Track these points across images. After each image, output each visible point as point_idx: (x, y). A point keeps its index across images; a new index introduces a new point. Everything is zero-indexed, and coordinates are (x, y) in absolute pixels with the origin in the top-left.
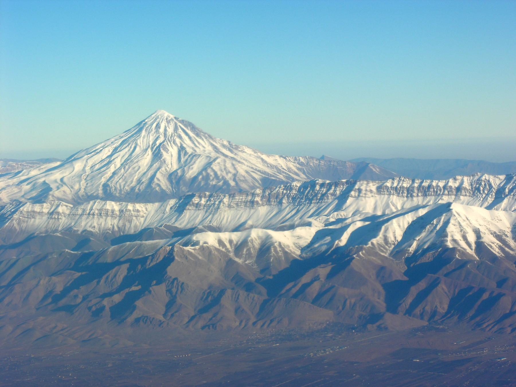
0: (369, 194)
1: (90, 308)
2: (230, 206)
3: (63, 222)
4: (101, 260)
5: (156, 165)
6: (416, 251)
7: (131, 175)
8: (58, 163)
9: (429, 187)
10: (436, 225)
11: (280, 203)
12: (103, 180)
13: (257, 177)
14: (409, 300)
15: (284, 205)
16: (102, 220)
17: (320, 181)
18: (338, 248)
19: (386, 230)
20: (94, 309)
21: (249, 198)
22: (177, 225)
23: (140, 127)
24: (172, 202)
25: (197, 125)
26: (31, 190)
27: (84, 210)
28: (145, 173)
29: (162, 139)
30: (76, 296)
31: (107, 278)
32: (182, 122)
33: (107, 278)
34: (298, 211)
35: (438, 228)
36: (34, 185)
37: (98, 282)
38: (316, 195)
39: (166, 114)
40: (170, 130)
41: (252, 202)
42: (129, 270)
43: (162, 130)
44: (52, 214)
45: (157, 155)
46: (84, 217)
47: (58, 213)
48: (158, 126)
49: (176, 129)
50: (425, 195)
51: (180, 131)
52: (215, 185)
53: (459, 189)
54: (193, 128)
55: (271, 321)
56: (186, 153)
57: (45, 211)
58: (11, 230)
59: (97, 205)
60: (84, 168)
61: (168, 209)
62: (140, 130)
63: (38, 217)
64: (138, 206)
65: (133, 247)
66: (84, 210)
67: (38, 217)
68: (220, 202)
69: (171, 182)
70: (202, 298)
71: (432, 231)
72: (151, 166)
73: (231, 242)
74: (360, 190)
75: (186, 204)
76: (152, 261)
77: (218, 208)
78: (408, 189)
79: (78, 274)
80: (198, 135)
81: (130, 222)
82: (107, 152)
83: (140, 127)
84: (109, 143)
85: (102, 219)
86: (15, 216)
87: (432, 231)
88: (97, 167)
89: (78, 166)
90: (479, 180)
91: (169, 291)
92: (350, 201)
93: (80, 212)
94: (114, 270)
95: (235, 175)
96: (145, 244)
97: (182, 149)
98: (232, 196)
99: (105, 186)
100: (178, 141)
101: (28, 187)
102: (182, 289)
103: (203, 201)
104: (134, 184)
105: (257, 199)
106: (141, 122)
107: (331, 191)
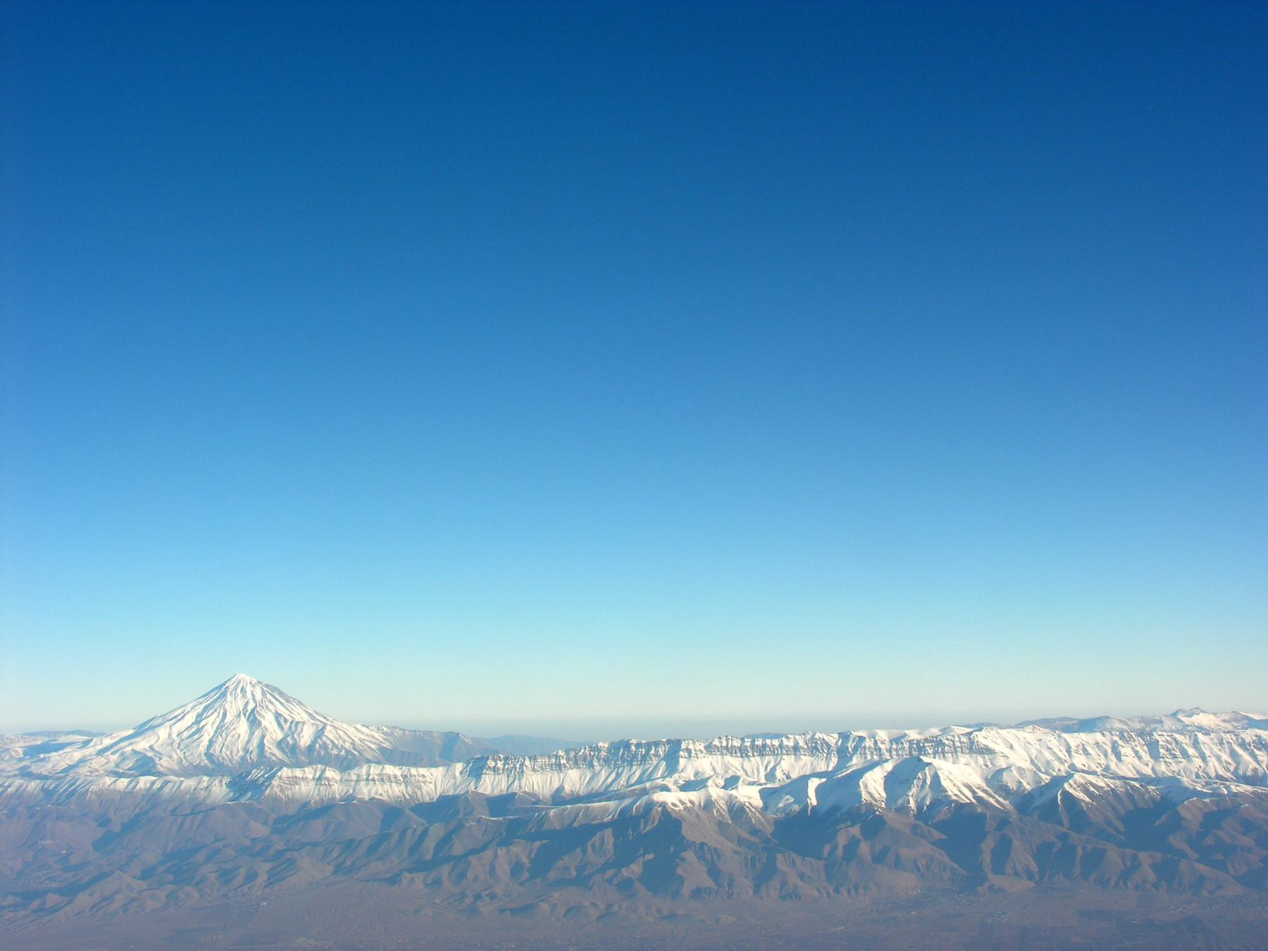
0: (700, 755)
1: (610, 881)
2: (534, 770)
3: (338, 790)
4: (546, 827)
5: (258, 733)
6: (919, 808)
7: (233, 744)
8: (131, 732)
9: (764, 746)
10: (924, 781)
11: (591, 765)
12: (202, 749)
13: (373, 746)
14: (987, 858)
15: (597, 768)
16: (387, 786)
17: (634, 741)
18: (814, 808)
19: (866, 787)
20: (615, 882)
21: (553, 760)
22: (480, 790)
23: (221, 692)
24: (459, 766)
25: (284, 691)
26: (122, 761)
27: (359, 776)
28: (248, 742)
29: (251, 706)
30: (566, 868)
31: (593, 845)
32: (267, 686)
33: (593, 845)
34: (618, 775)
35: (928, 782)
36: (122, 754)
37: (584, 851)
38: (635, 756)
39: (248, 679)
40: (259, 696)
41: (560, 765)
42: (615, 835)
43: (249, 695)
44: (320, 779)
45: (254, 722)
46: (363, 783)
47: (328, 779)
48: (243, 690)
49: (264, 693)
50: (762, 755)
51: (269, 696)
52: (337, 756)
53: (796, 748)
54: (281, 693)
55: (856, 888)
56: (286, 721)
57: (310, 776)
58: (276, 799)
59: (375, 770)
60: (170, 735)
61: (457, 774)
62: (224, 695)
63: (302, 784)
64: (422, 771)
65: (579, 810)
66: (359, 776)
67: (302, 784)
68: (522, 765)
69: (283, 751)
70: (746, 865)
71: (923, 787)
72: (252, 734)
73: (691, 802)
74: (689, 751)
75: (482, 768)
76: (646, 823)
77: (523, 772)
78: (740, 749)
79: (538, 844)
80: (287, 701)
81: (420, 788)
82: (190, 719)
83: (221, 692)
84: (188, 708)
85: (384, 784)
86: (275, 782)
87: (923, 787)
88: (186, 734)
89: (163, 733)
90: (813, 738)
91: (701, 858)
92: (682, 762)
93: (354, 777)
94: (596, 838)
95: (353, 743)
96: (594, 809)
97: (278, 716)
98: (533, 758)
99: (209, 755)
100: (270, 706)
101: (115, 757)
102: (718, 856)
103: (500, 764)
104: (241, 753)
105: (563, 761)
106: (220, 687)
107: (653, 752)
